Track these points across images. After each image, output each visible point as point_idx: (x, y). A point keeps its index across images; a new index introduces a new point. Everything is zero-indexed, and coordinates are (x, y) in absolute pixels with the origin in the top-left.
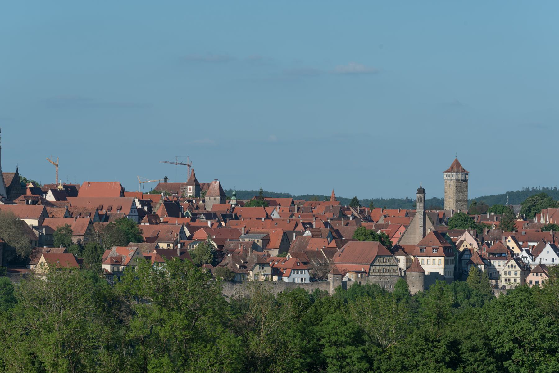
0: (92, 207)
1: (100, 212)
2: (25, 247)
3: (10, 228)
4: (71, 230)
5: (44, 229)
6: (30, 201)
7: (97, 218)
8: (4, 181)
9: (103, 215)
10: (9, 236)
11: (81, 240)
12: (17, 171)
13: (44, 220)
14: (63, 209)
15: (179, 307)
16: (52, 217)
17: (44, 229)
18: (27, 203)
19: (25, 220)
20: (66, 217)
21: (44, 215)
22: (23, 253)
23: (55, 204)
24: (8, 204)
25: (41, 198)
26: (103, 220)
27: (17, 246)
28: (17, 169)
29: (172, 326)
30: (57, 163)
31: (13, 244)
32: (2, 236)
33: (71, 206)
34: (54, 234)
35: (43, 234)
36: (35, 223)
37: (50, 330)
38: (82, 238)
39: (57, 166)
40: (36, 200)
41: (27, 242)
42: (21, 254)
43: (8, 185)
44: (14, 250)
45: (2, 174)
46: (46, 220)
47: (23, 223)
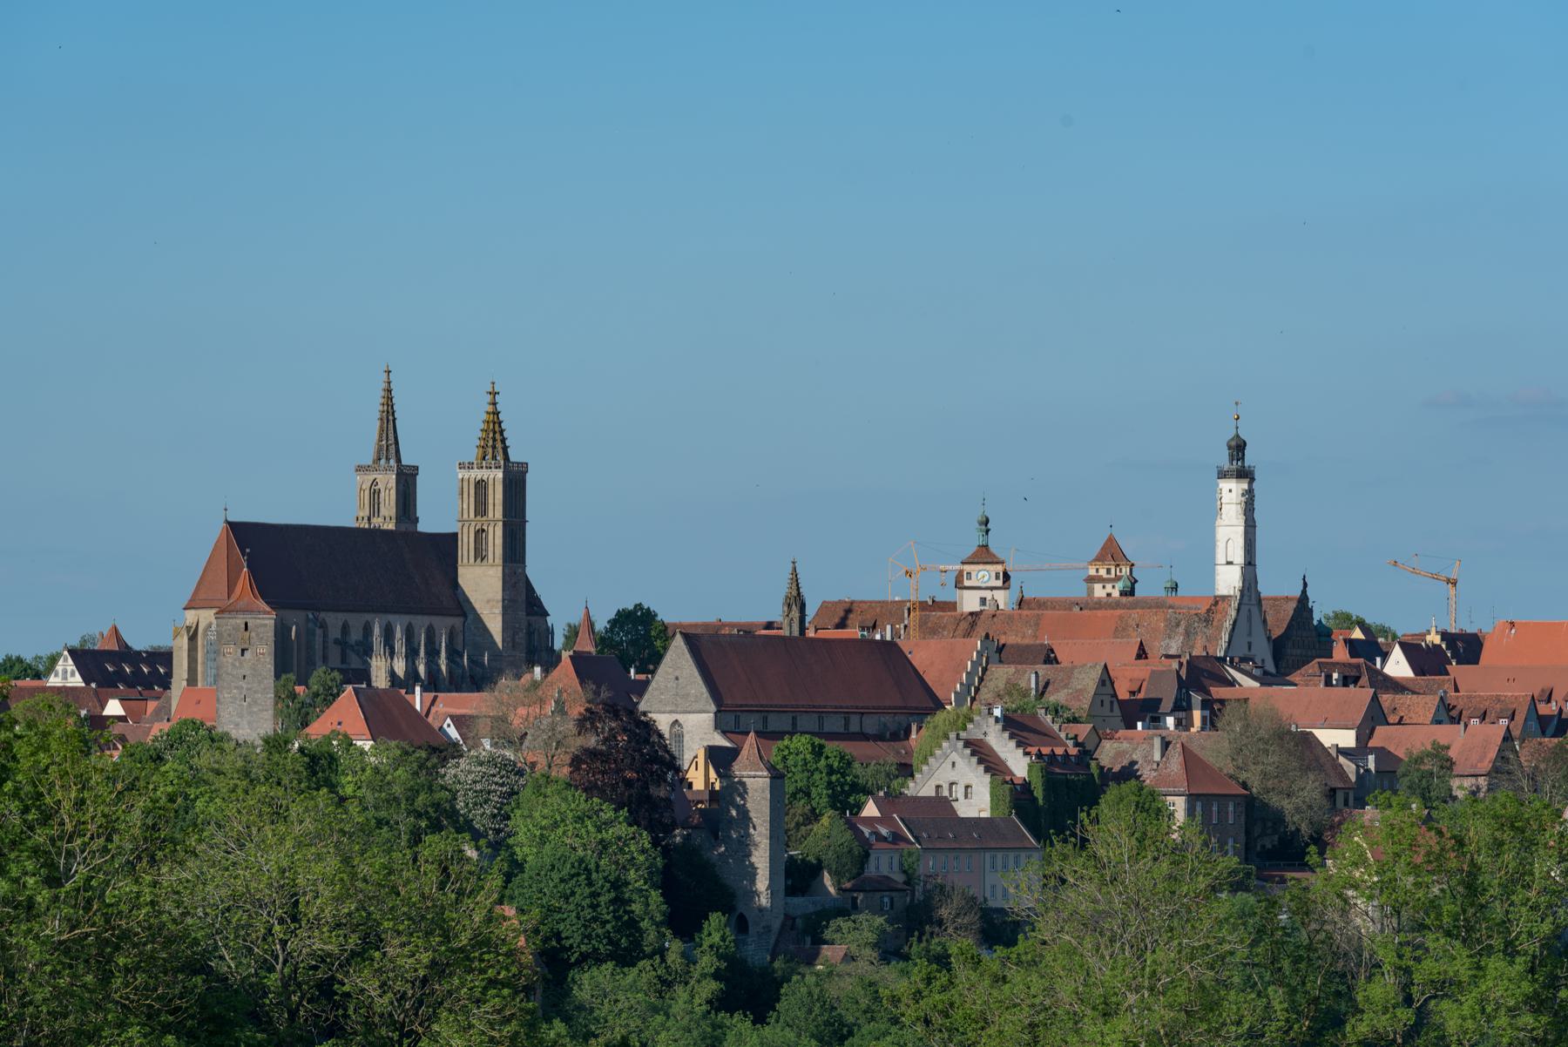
0: (1518, 694)
1: (1543, 709)
2: (1310, 807)
3: (1266, 752)
4: (1449, 760)
5: (1371, 758)
6: (1335, 676)
7: (1534, 725)
8: (1265, 621)
9: (1552, 717)
10: (1265, 774)
11: (1478, 789)
12: (1304, 591)
13: (1372, 731)
14: (1428, 698)
15: (1508, 944)
16: (1399, 723)
17: (1371, 758)
18: (1328, 683)
19: (1316, 732)
20: (1439, 722)
21: (1374, 717)
22: (1304, 827)
23: (1411, 686)
24: (1270, 685)
25: (1368, 668)
26: (1551, 729)
27: (1287, 805)
28: (1305, 585)
29: (1482, 1001)
30: (1452, 576)
31: (1275, 800)
32: (1243, 776)
33: (1457, 690)
34: (1401, 770)
35: (1368, 771)
36: (1347, 739)
37: (1108, 1012)
38: (1482, 781)
39: (1454, 584)
40: (1354, 673)
41: (1317, 795)
42: (1298, 830)
43: (1277, 632)
44: (1278, 818)
45: (1260, 601)
46: (1380, 731)
47: (1309, 741)
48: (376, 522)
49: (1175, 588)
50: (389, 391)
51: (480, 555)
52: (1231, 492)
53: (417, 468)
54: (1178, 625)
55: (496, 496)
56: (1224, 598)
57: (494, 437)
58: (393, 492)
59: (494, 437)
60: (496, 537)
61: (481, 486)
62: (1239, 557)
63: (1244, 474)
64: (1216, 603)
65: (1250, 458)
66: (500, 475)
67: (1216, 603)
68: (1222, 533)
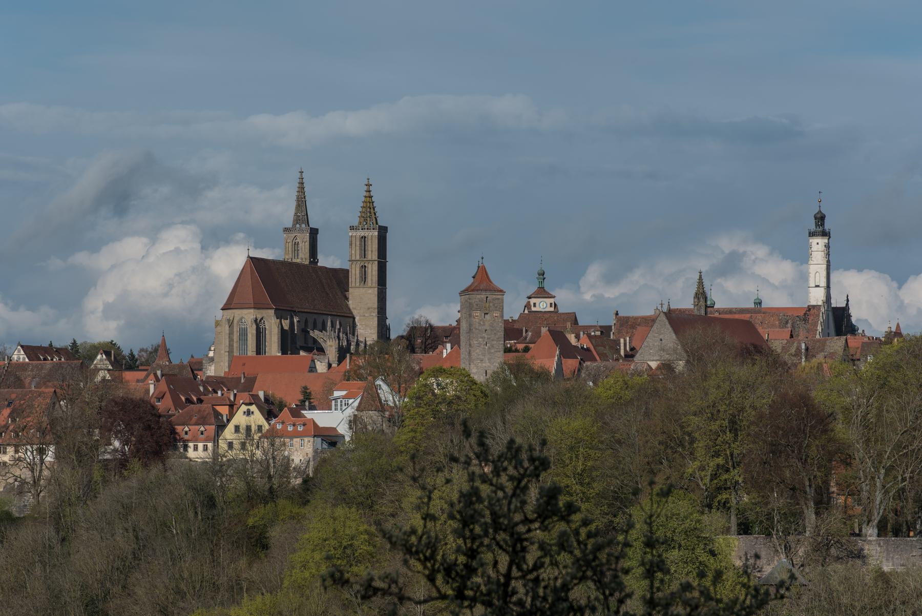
12: (847, 304)
28: (848, 300)
48: (294, 261)
49: (760, 303)
50: (303, 184)
51: (364, 278)
52: (818, 244)
53: (317, 230)
54: (787, 322)
55: (373, 247)
56: (814, 306)
57: (369, 210)
58: (307, 244)
59: (369, 210)
60: (372, 270)
61: (364, 238)
62: (823, 283)
63: (825, 234)
64: (809, 310)
65: (827, 227)
66: (376, 234)
67: (809, 310)
68: (813, 269)
